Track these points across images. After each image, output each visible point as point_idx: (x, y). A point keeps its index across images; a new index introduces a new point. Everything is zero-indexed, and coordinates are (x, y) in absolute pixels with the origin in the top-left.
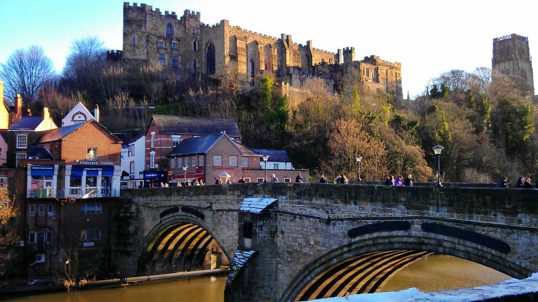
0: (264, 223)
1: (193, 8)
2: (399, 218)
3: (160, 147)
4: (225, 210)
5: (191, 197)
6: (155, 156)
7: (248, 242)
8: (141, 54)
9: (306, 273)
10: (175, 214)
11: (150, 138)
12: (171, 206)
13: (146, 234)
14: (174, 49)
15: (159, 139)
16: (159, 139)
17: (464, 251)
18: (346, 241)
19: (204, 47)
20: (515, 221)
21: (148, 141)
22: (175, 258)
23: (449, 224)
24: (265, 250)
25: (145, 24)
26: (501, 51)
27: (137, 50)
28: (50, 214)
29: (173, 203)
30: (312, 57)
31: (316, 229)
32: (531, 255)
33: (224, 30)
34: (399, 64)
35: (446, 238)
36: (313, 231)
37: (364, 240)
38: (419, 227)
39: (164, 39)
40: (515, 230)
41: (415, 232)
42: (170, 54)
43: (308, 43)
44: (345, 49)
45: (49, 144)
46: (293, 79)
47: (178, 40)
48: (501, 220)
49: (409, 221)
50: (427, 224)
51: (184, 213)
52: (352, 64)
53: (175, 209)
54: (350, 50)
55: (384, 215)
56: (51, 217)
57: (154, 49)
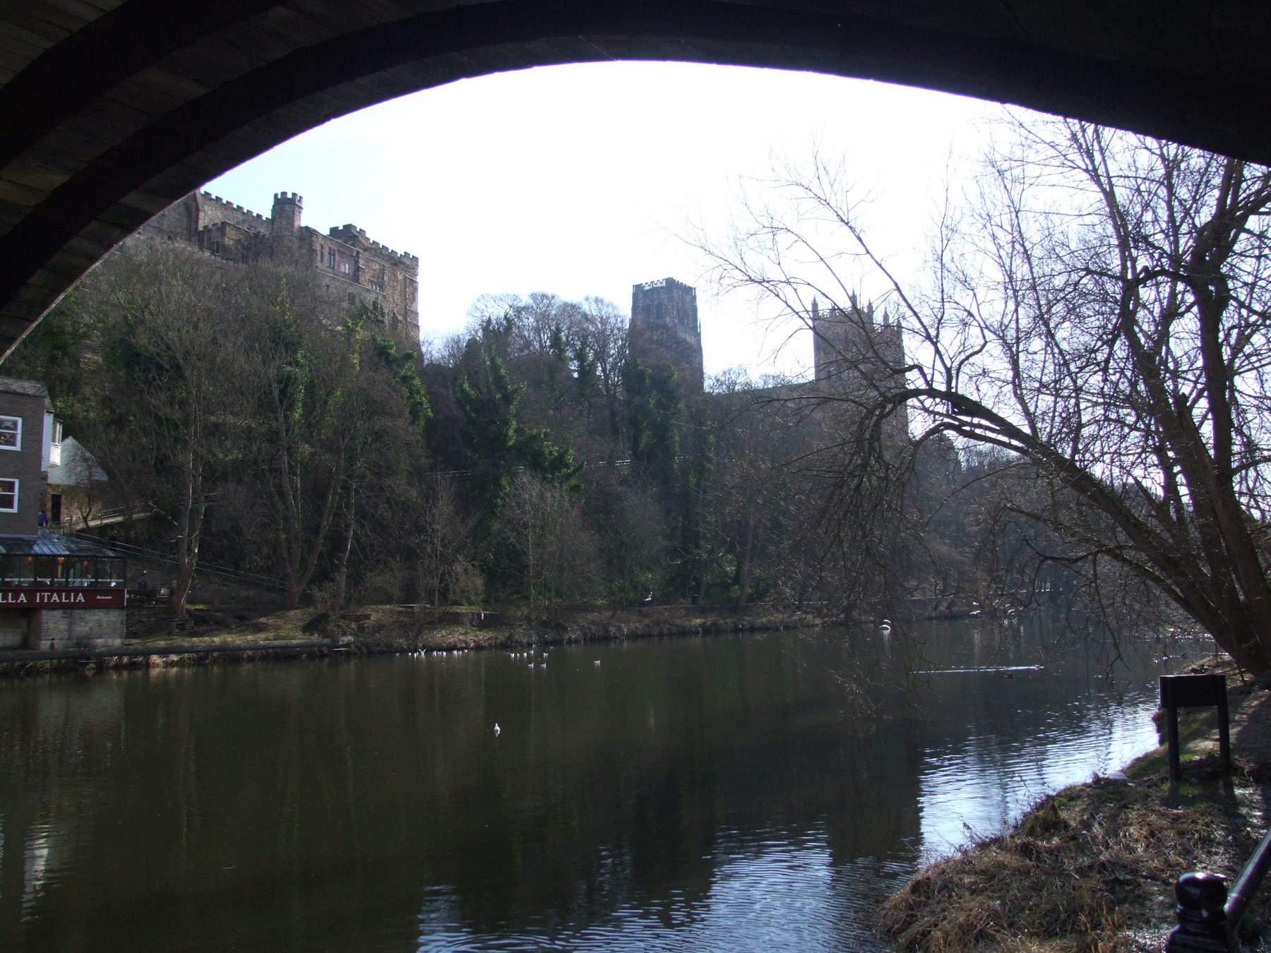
26: (647, 309)
30: (198, 210)
34: (415, 259)
44: (279, 197)
54: (289, 199)
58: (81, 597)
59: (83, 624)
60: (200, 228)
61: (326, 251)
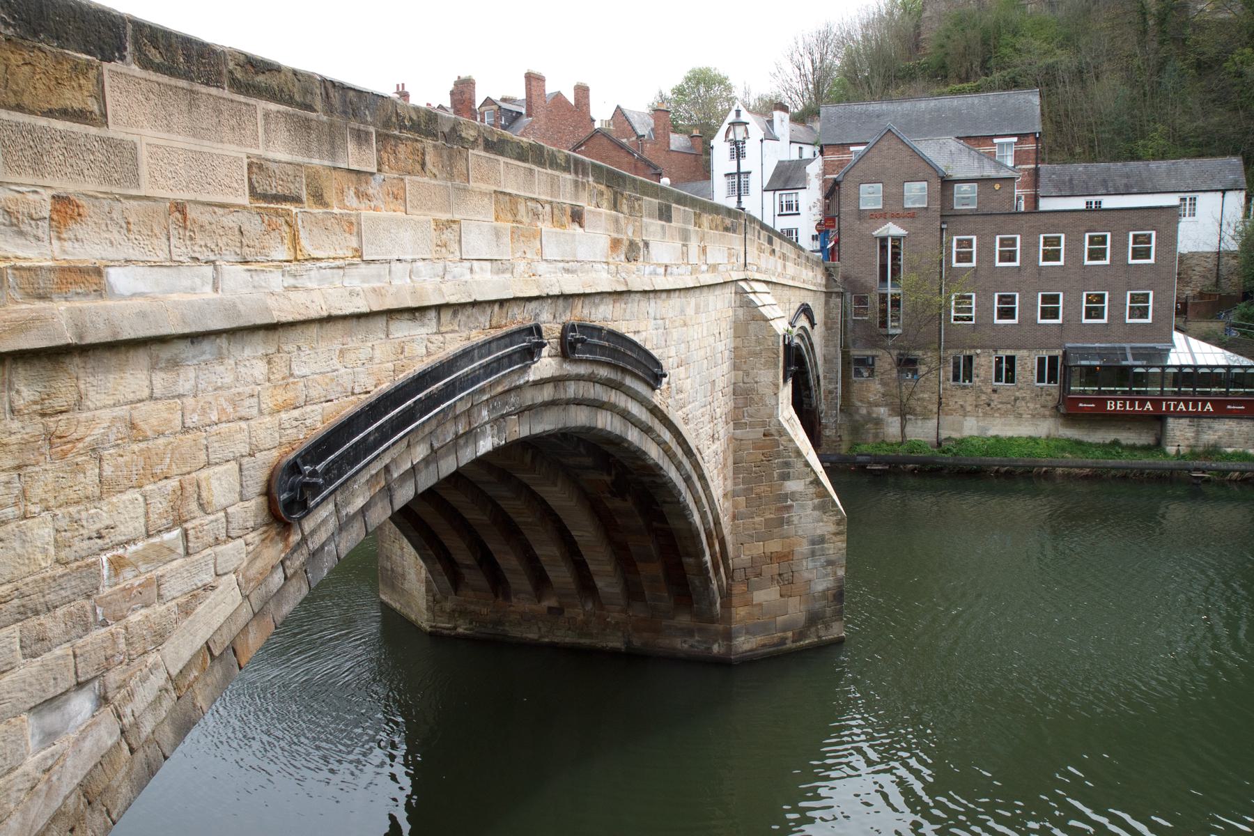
58: (1209, 407)
59: (1210, 432)
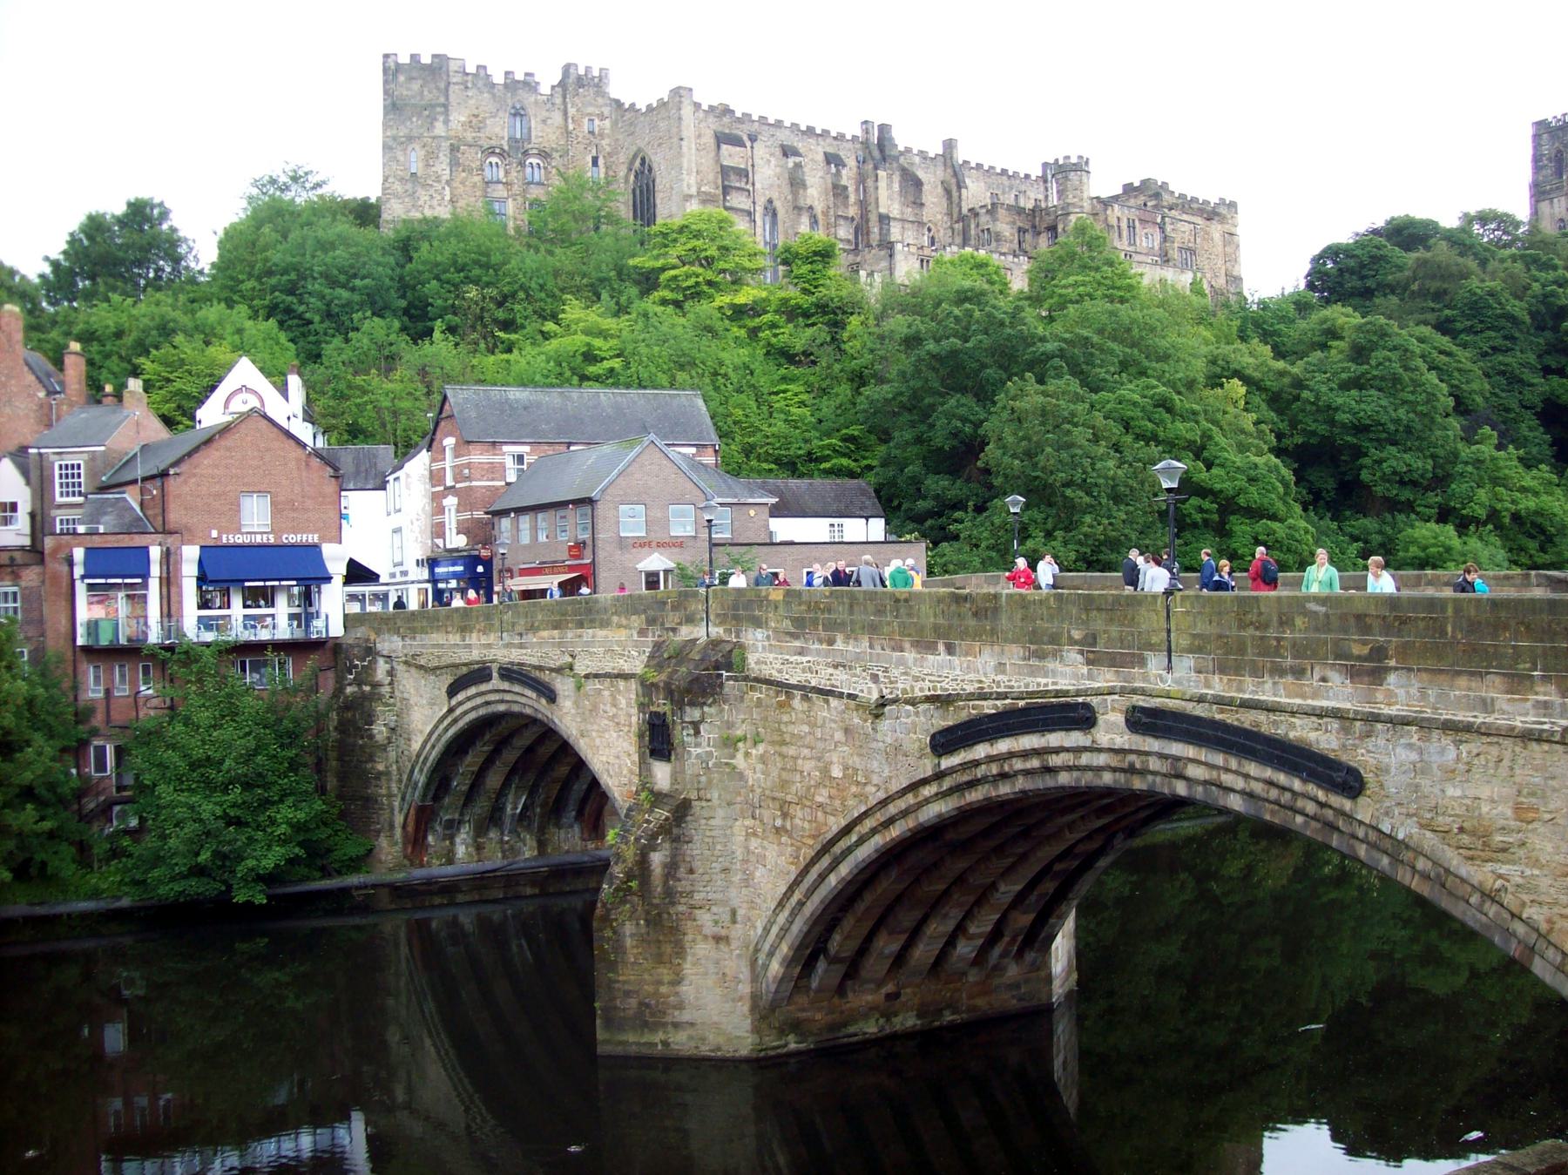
0: (703, 713)
1: (587, 60)
2: (1065, 693)
3: (467, 484)
4: (607, 675)
5: (521, 635)
6: (458, 511)
7: (662, 774)
8: (435, 202)
9: (826, 861)
10: (483, 687)
11: (441, 457)
12: (471, 663)
13: (416, 746)
14: (532, 183)
15: (464, 460)
16: (464, 460)
17: (1243, 793)
18: (927, 767)
19: (622, 173)
20: (1380, 696)
21: (436, 466)
22: (513, 815)
23: (1199, 711)
24: (708, 797)
25: (446, 113)
27: (421, 192)
28: (146, 690)
29: (475, 655)
31: (847, 731)
32: (1423, 802)
33: (680, 118)
34: (1232, 206)
35: (1190, 751)
36: (839, 736)
37: (976, 763)
38: (1119, 718)
39: (502, 154)
40: (1379, 726)
41: (1109, 736)
42: (520, 199)
43: (949, 145)
45: (136, 489)
46: (898, 257)
47: (544, 154)
48: (1340, 693)
49: (1094, 701)
50: (1143, 710)
51: (506, 686)
52: (1082, 207)
53: (479, 674)
55: (1027, 685)
56: (148, 698)
57: (475, 185)
60: (965, 211)
61: (1124, 225)
